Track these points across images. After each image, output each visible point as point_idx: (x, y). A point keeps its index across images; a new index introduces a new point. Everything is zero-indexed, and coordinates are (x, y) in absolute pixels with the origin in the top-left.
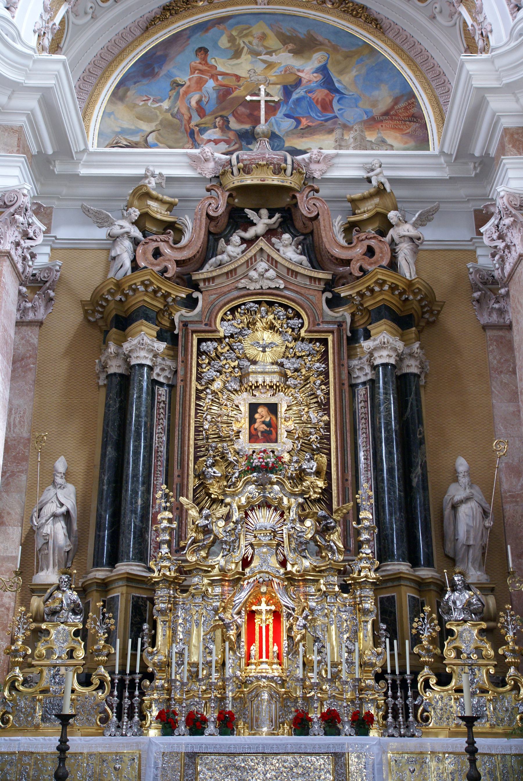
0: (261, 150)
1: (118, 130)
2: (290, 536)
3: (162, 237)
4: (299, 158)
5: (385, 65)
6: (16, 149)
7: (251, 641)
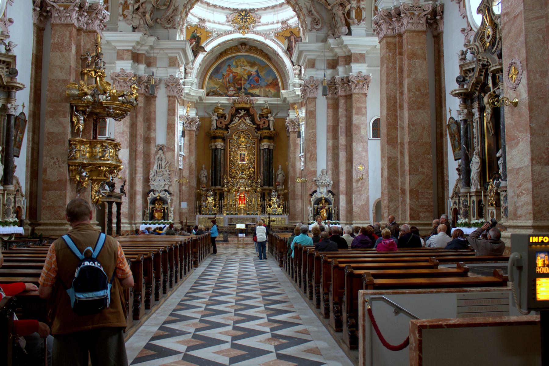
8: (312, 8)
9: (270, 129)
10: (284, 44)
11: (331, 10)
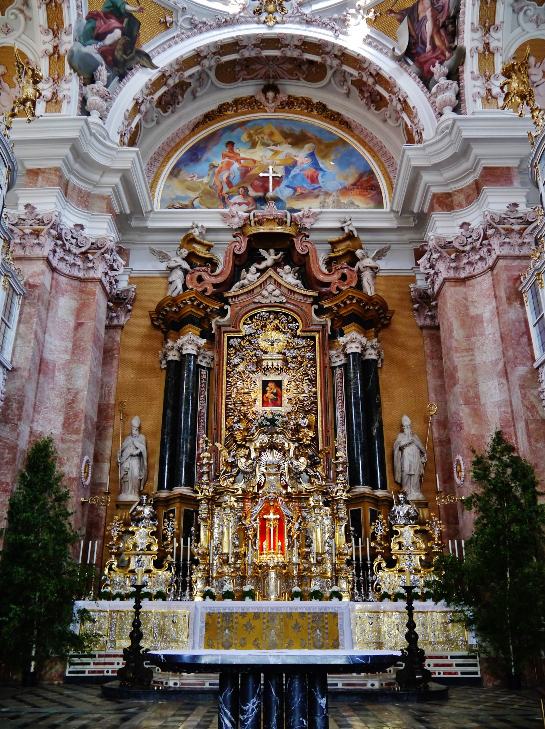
0: (270, 210)
1: (174, 197)
2: (290, 469)
3: (203, 268)
4: (296, 214)
5: (353, 153)
6: (105, 210)
7: (263, 539)
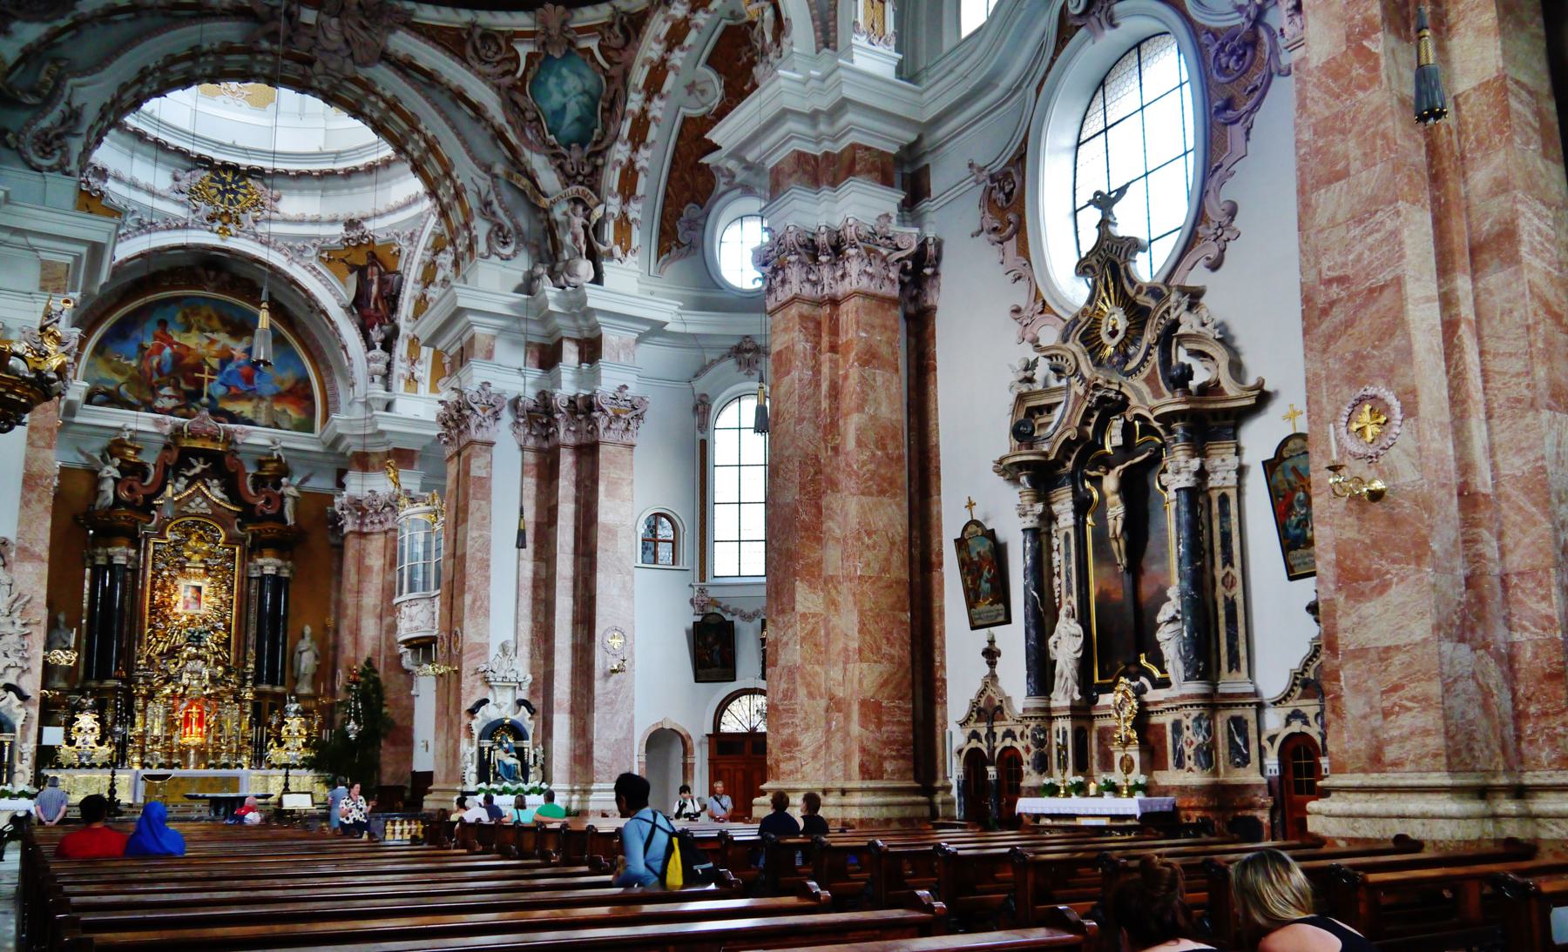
5: (293, 353)
8: (492, 197)
9: (285, 521)
10: (344, 283)
11: (547, 211)
